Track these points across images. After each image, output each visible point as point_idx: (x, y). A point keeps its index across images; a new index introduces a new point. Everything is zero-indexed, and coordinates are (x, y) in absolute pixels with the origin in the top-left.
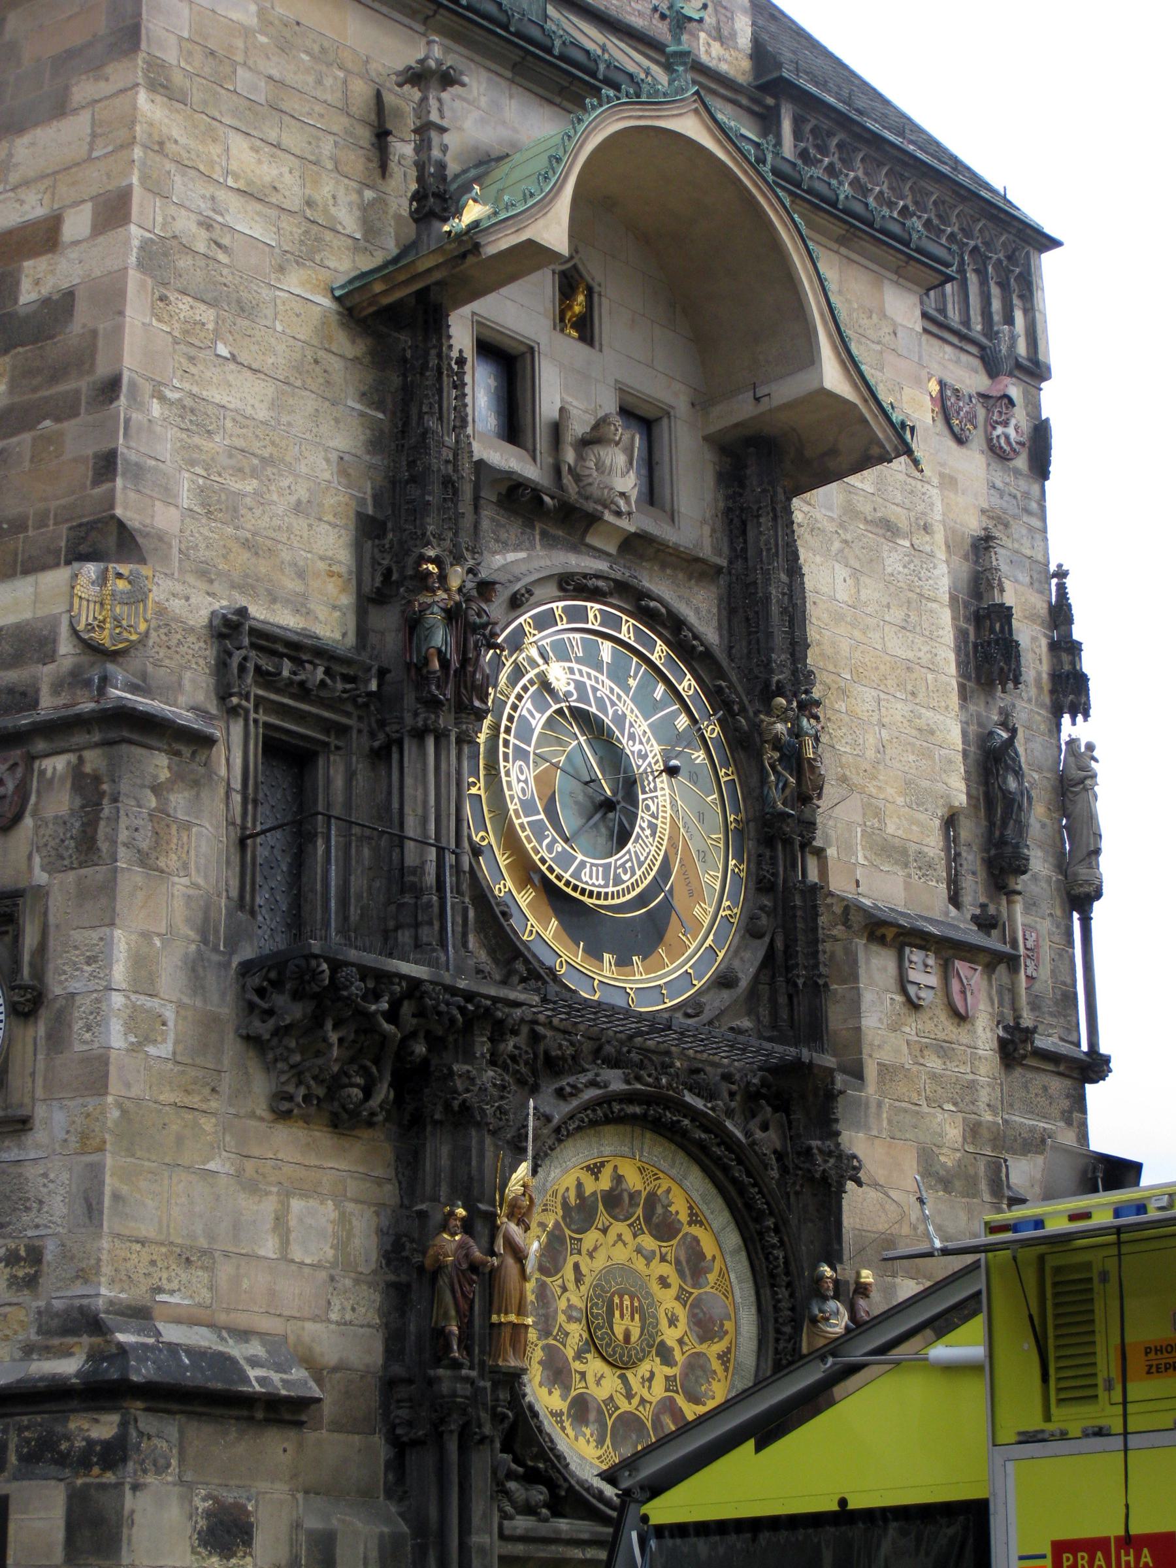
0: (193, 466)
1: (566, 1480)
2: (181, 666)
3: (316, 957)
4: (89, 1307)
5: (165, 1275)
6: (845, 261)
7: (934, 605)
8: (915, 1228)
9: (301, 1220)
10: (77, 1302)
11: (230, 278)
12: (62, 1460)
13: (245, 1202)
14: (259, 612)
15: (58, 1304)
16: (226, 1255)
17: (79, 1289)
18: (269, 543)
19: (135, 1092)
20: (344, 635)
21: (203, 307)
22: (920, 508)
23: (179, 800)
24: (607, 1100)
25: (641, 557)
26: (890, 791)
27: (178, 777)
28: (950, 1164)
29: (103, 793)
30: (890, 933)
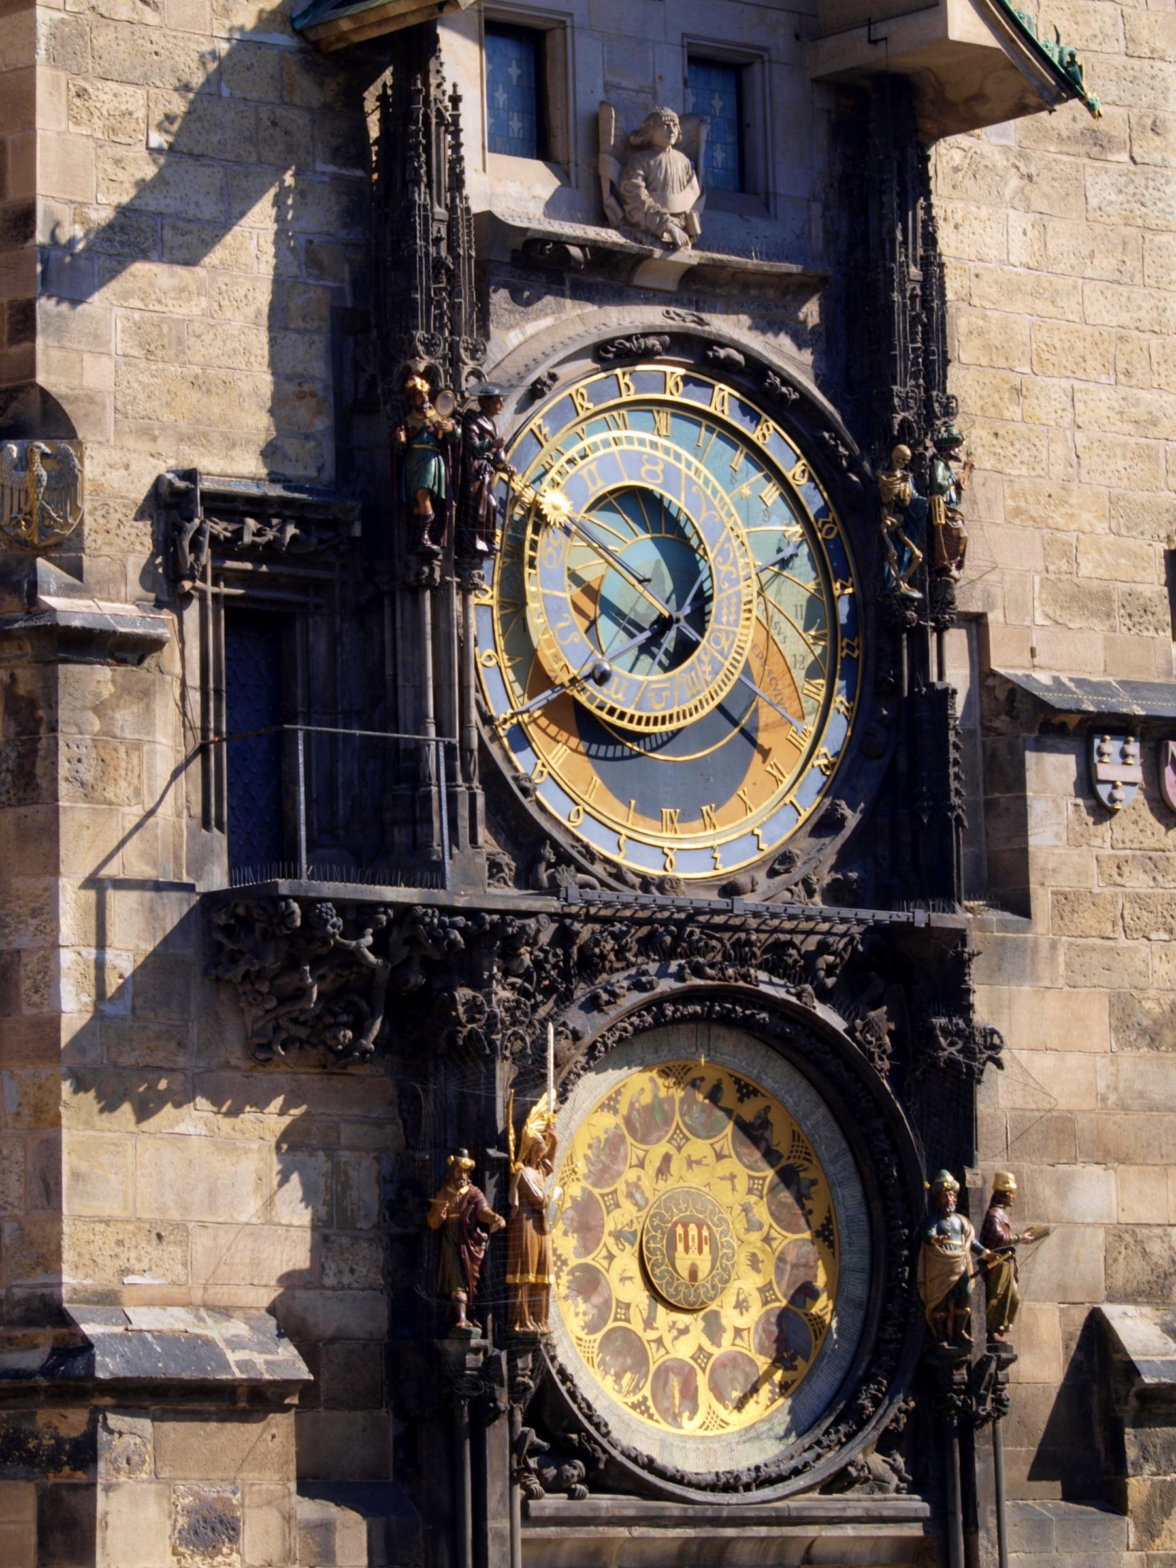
0: (126, 300)
1: (605, 1451)
2: (122, 551)
3: (285, 898)
4: (51, 1295)
5: (133, 1255)
8: (1104, 1099)
10: (39, 1291)
11: (162, 42)
12: (31, 1459)
15: (18, 1293)
16: (203, 1225)
17: (40, 1278)
18: (223, 374)
20: (320, 469)
21: (130, 89)
23: (125, 718)
26: (1086, 518)
27: (124, 691)
29: (39, 721)
30: (1072, 721)
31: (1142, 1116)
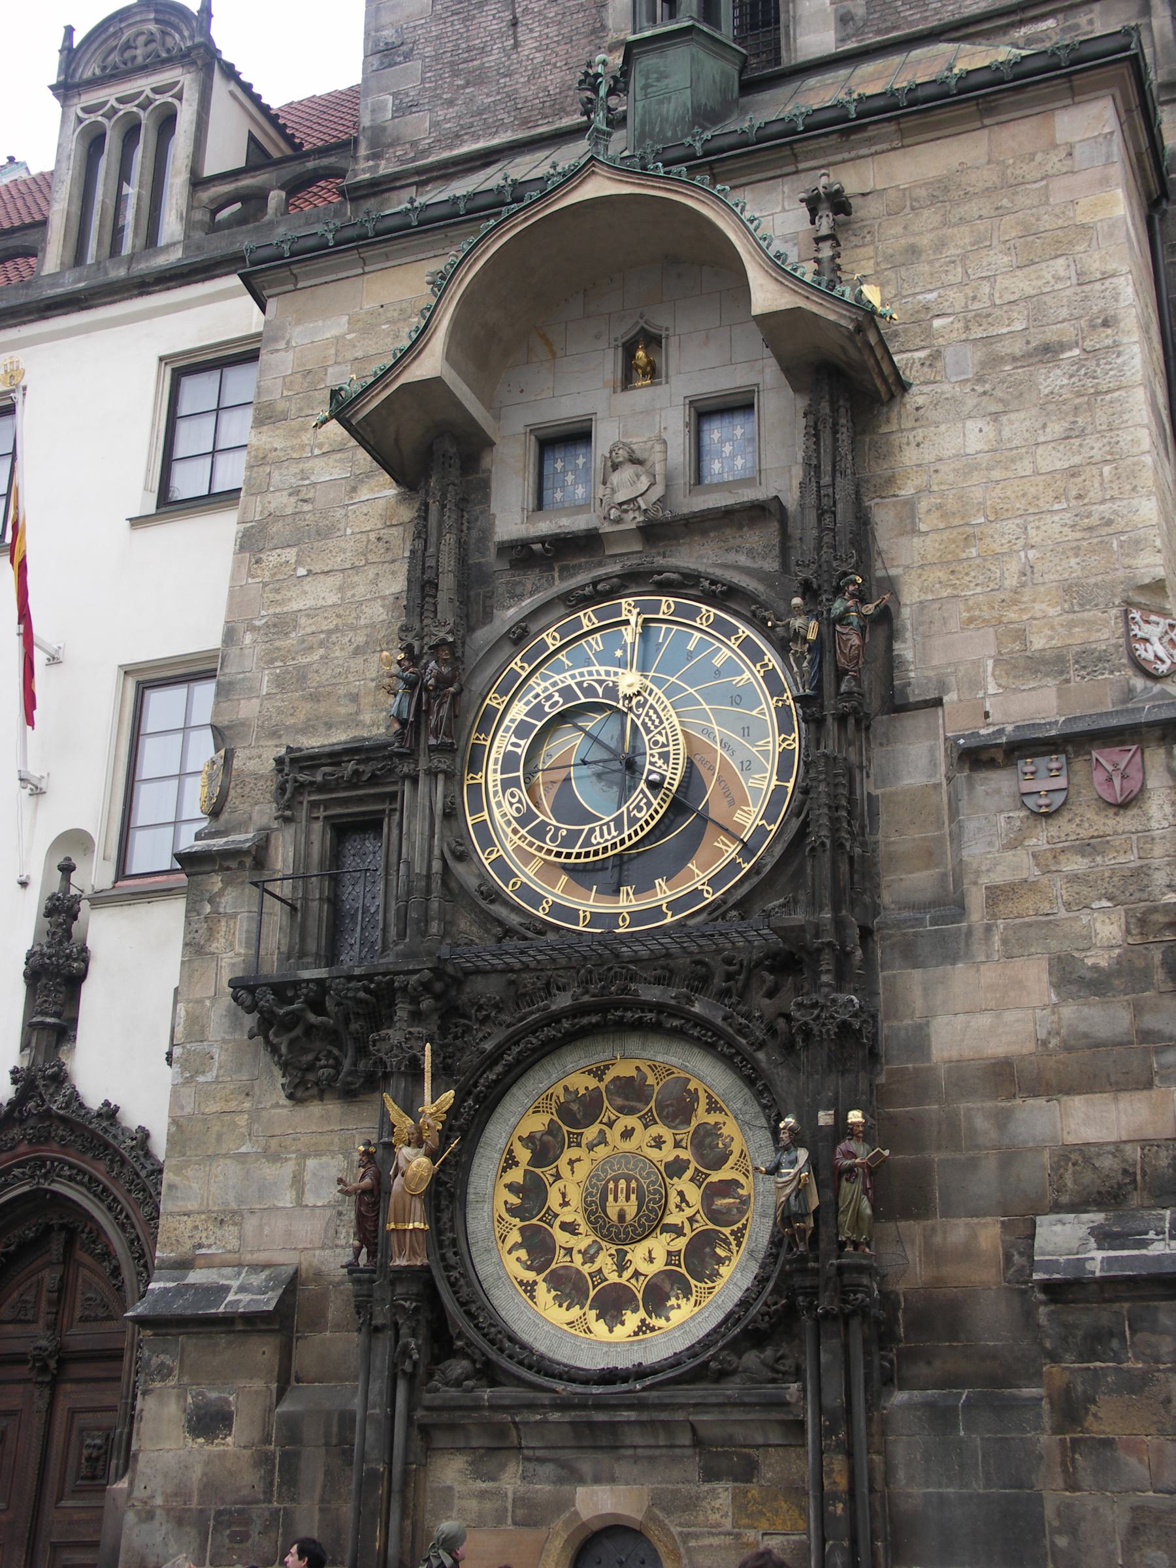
1: (483, 1354)
6: (996, 128)
7: (1116, 394)
8: (1045, 1043)
9: (314, 1174)
13: (269, 1171)
14: (313, 742)
18: (328, 689)
19: (188, 1110)
20: (388, 728)
22: (1095, 309)
24: (554, 1019)
25: (676, 537)
27: (227, 883)
28: (1103, 963)
30: (1000, 757)
31: (1088, 1052)
